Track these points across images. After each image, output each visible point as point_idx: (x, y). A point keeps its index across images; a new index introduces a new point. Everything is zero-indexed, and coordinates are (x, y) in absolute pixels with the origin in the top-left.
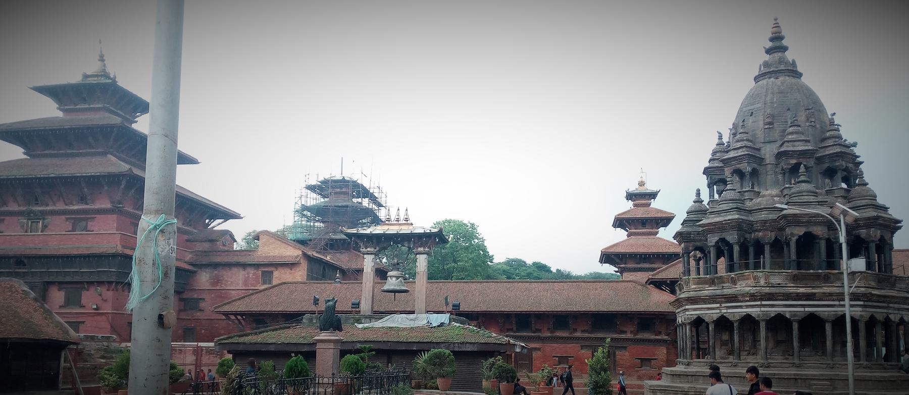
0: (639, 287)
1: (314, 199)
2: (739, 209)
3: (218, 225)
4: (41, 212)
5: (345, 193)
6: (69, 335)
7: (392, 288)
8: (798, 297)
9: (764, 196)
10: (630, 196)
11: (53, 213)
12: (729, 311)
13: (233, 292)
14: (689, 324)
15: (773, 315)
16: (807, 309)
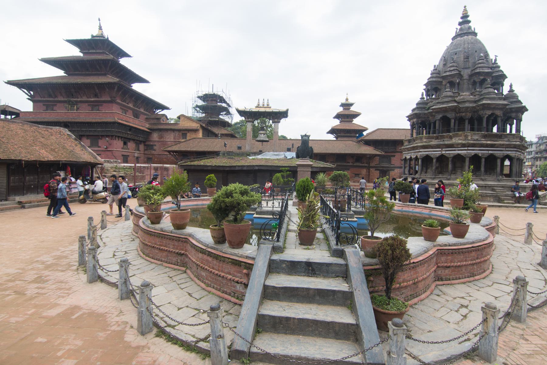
0: (355, 143)
1: (200, 103)
2: (455, 101)
3: (160, 112)
4: (75, 101)
5: (215, 100)
6: (97, 159)
7: (262, 139)
8: (487, 146)
9: (462, 95)
10: (342, 105)
11: (81, 102)
12: (447, 152)
13: (169, 142)
14: (421, 158)
15: (473, 155)
16: (490, 152)
